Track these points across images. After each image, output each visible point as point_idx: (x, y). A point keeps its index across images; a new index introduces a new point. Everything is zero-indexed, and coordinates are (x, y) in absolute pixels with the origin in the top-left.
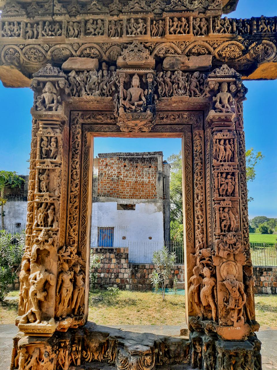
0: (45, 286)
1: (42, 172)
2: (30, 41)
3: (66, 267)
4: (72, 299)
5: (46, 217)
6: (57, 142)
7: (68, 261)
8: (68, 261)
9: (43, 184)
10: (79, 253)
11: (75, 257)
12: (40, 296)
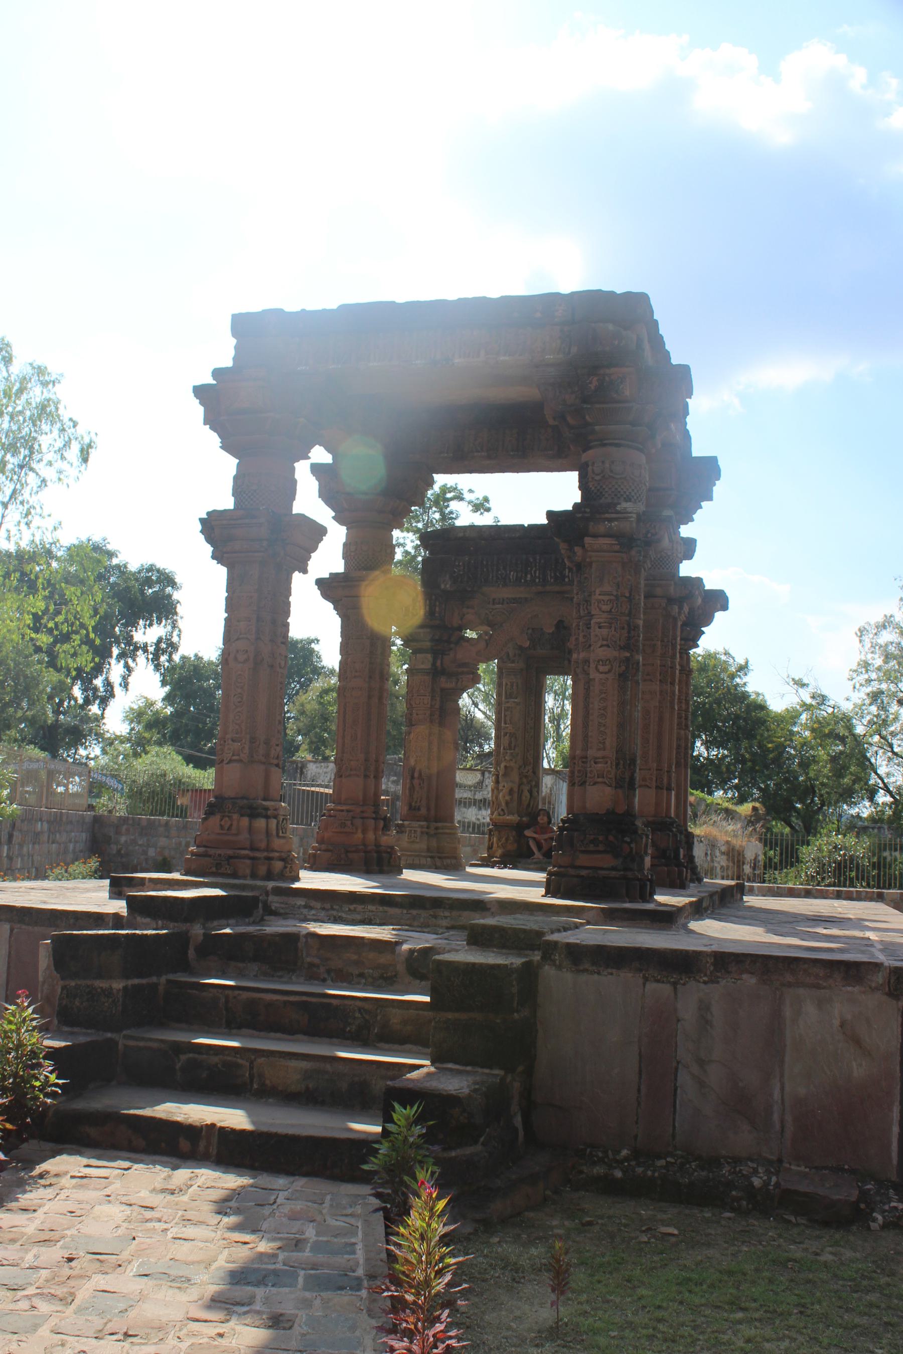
0: (511, 792)
1: (507, 709)
2: (497, 606)
3: (524, 780)
4: (529, 805)
5: (510, 743)
6: (517, 686)
7: (526, 777)
8: (526, 777)
9: (508, 719)
10: (534, 773)
11: (530, 773)
12: (508, 798)
